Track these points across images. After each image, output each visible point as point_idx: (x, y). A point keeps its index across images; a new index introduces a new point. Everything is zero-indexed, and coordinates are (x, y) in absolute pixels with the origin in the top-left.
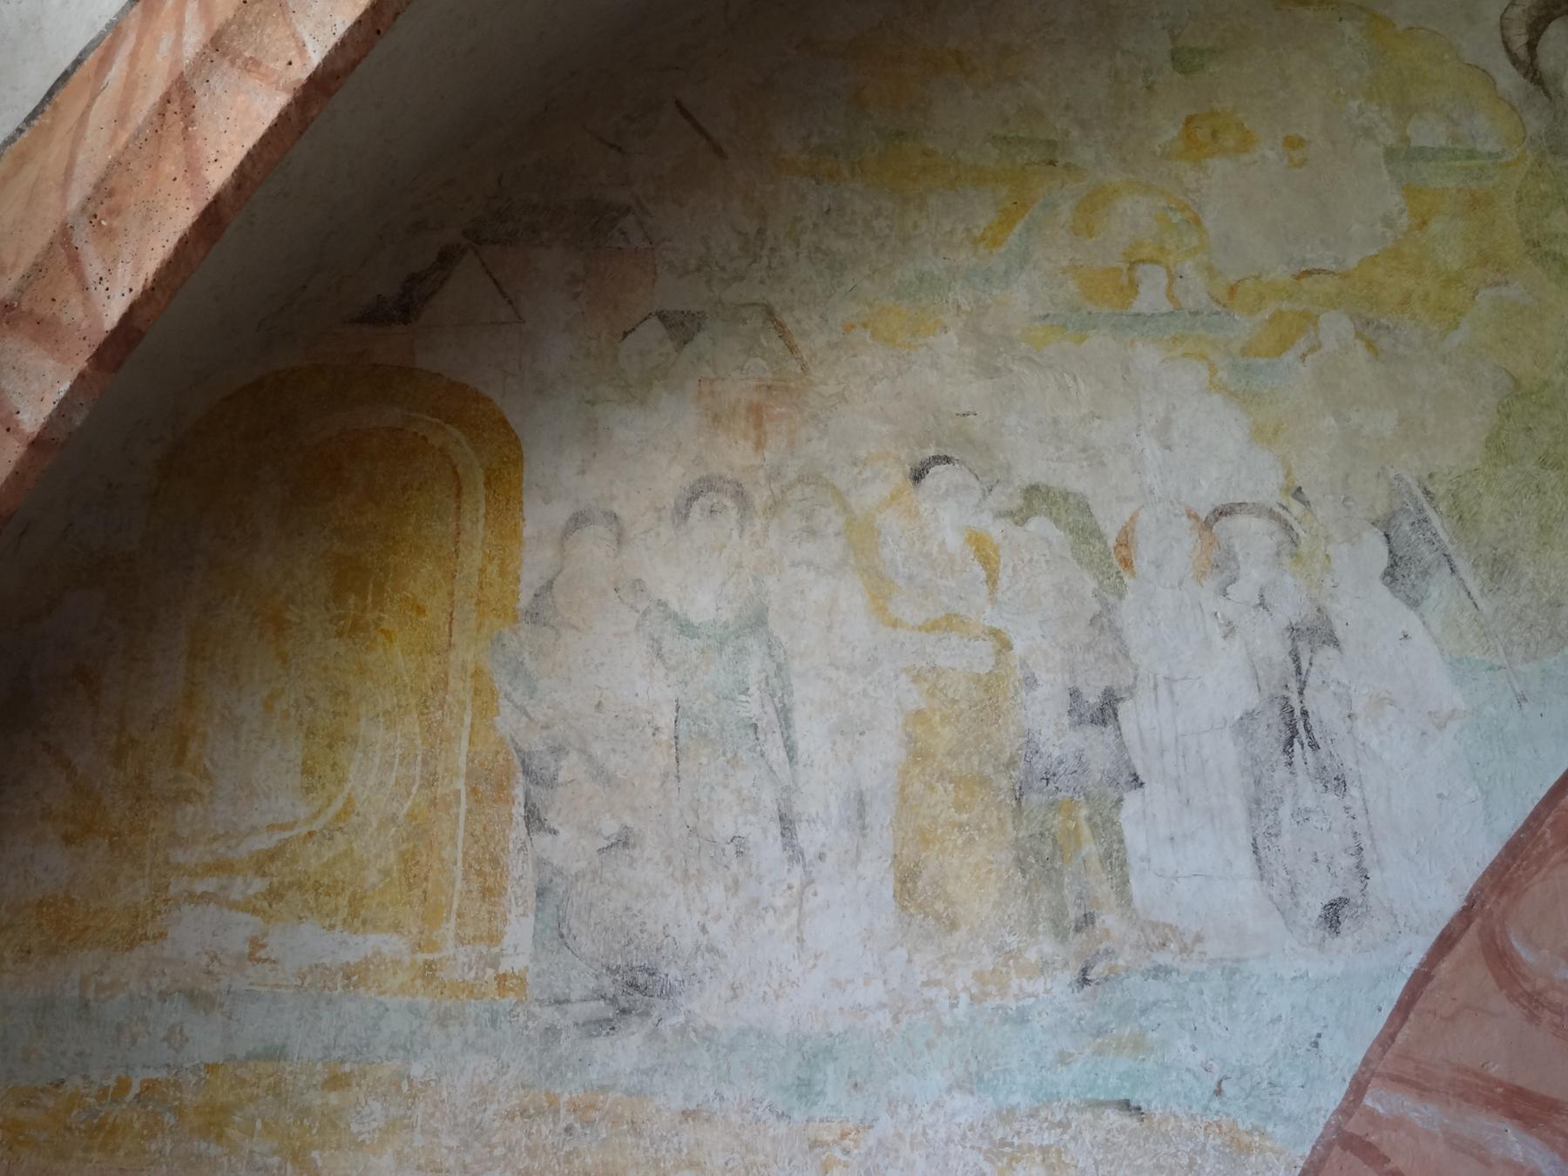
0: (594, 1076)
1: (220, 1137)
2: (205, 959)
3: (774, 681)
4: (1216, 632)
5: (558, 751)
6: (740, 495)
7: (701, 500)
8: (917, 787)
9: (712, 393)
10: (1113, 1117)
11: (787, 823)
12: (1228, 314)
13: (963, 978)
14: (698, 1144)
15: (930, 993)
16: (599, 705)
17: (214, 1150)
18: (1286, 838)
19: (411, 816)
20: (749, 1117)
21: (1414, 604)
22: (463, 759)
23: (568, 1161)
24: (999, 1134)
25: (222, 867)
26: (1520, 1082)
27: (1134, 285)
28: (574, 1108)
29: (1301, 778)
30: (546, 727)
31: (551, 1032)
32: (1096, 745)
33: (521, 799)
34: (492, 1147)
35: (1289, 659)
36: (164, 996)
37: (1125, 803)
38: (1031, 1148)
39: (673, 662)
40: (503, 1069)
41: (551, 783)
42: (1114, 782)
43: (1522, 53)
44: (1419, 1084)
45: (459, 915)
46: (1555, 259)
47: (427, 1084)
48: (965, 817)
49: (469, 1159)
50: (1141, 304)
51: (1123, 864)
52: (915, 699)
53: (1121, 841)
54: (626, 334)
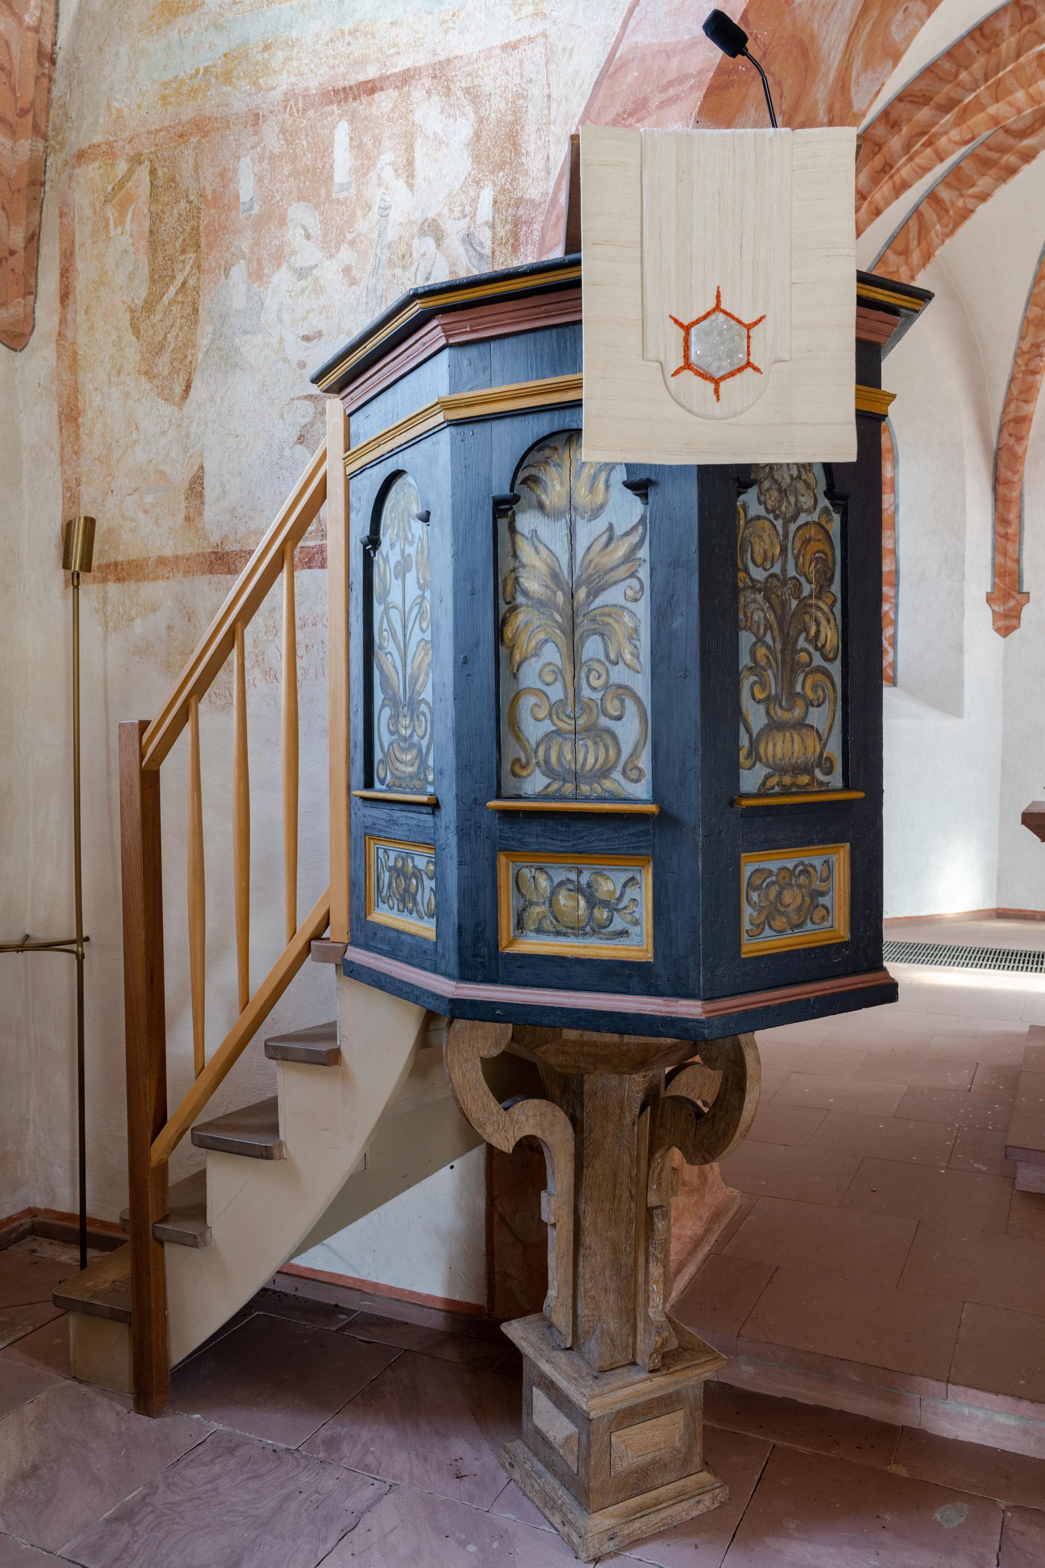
1: (230, 82)
14: (397, 36)
17: (229, 89)
28: (350, 33)
34: (321, 59)
36: (206, 29)
47: (297, 39)
49: (312, 66)
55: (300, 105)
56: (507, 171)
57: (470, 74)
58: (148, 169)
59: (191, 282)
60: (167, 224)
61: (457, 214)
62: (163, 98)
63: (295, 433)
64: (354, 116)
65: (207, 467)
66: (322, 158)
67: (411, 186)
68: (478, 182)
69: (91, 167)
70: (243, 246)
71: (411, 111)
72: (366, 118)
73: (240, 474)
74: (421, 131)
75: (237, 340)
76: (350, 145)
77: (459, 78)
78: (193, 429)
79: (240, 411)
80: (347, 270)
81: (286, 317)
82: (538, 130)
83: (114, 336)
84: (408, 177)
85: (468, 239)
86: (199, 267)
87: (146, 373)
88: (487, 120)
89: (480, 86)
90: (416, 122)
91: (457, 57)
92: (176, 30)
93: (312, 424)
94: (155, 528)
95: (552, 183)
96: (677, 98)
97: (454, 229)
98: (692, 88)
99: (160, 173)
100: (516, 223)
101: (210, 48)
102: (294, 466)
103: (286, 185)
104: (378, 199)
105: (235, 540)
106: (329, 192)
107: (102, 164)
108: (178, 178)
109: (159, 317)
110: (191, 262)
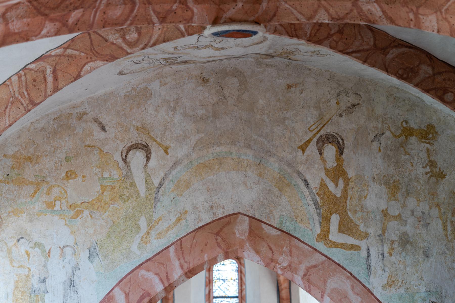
8: (16, 293)
18: (68, 301)
21: (92, 262)
27: (55, 205)
29: (72, 291)
32: (42, 286)
35: (72, 272)
37: (46, 295)
42: (44, 292)
43: (124, 158)
48: (22, 297)
50: (55, 209)
52: (16, 279)
53: (45, 301)
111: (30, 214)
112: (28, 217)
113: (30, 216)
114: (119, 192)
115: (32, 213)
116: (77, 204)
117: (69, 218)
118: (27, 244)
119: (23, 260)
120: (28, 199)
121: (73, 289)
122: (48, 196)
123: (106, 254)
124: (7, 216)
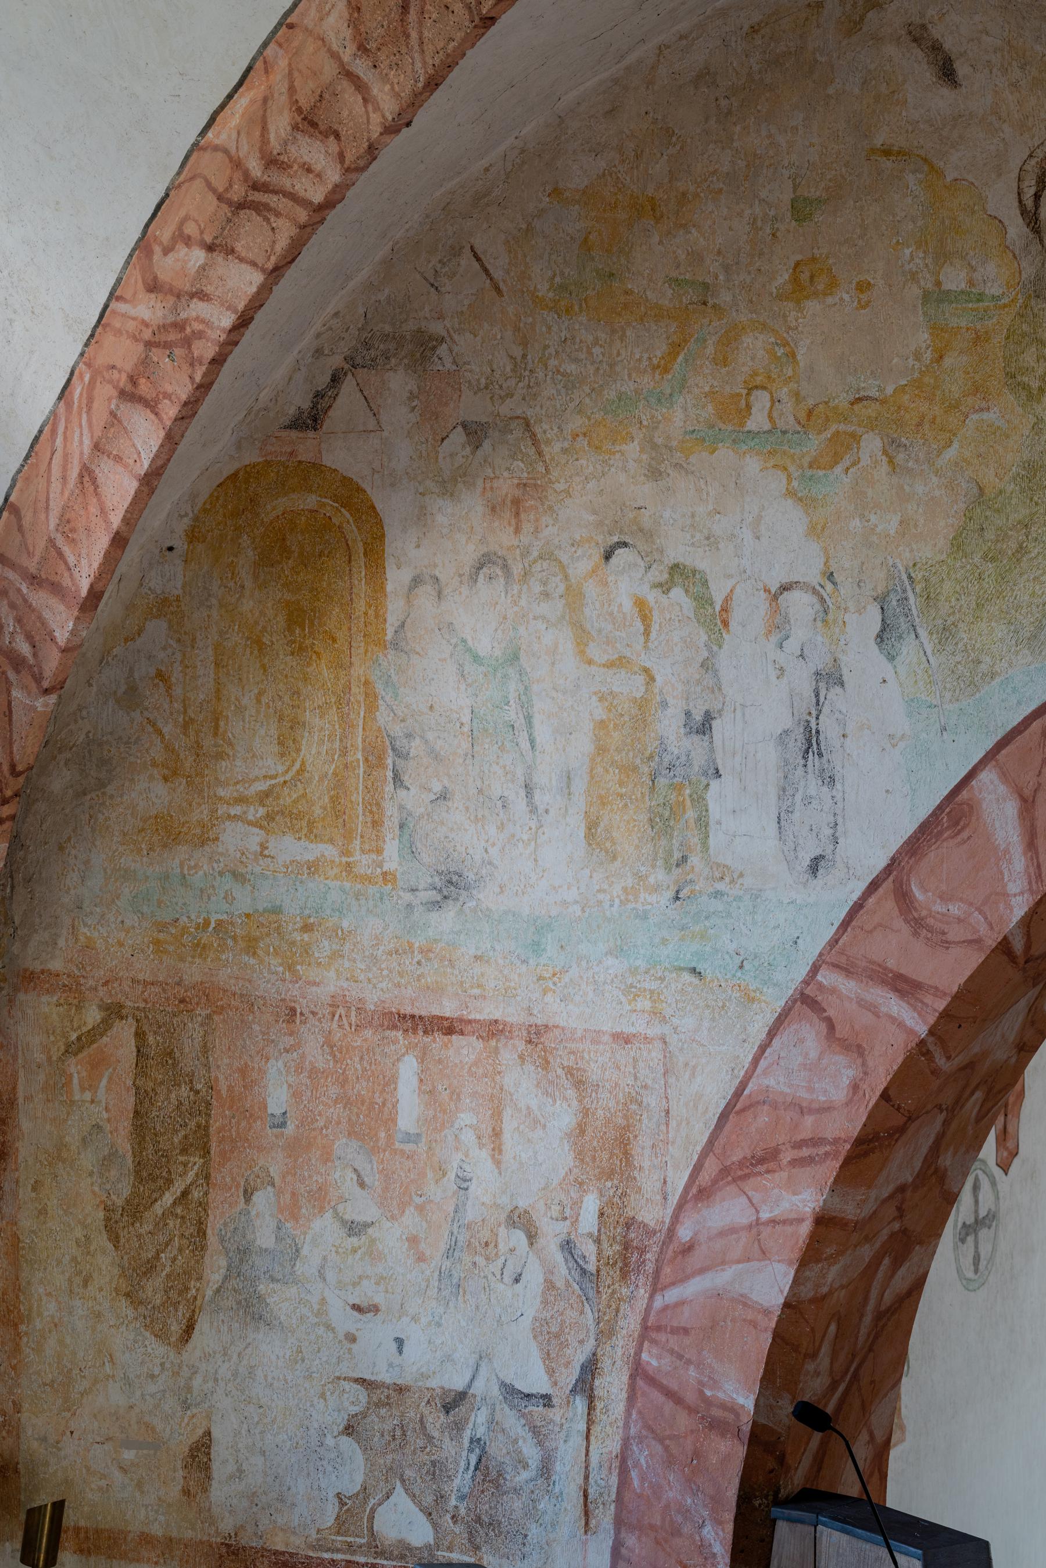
0: (431, 934)
1: (254, 953)
2: (239, 855)
3: (523, 698)
4: (773, 674)
5: (409, 736)
6: (506, 567)
7: (485, 569)
8: (599, 770)
9: (492, 488)
10: (687, 977)
11: (529, 789)
12: (805, 433)
13: (617, 890)
15: (601, 896)
16: (431, 707)
17: (252, 961)
18: (796, 816)
19: (335, 774)
20: (507, 961)
21: (891, 658)
22: (360, 739)
23: (419, 980)
24: (629, 981)
25: (241, 800)
26: (902, 971)
29: (810, 776)
30: (403, 721)
31: (409, 906)
32: (697, 746)
33: (391, 767)
34: (382, 970)
35: (813, 695)
36: (221, 874)
37: (711, 787)
38: (645, 990)
39: (469, 681)
40: (386, 927)
41: (405, 757)
42: (705, 774)
44: (848, 970)
45: (362, 837)
46: (1024, 388)
49: (371, 976)
51: (707, 825)
52: (600, 713)
53: (707, 811)
54: (443, 440)
55: (353, 1019)
56: (615, 1182)
57: (573, 1053)
58: (133, 1030)
59: (196, 1194)
60: (160, 1109)
61: (555, 1214)
62: (157, 942)
63: (342, 1421)
64: (425, 1054)
65: (214, 1434)
66: (381, 1093)
67: (498, 1163)
68: (581, 1184)
69: (45, 999)
70: (271, 1169)
71: (499, 1073)
72: (440, 1061)
73: (263, 1453)
74: (512, 1100)
75: (262, 1286)
76: (419, 1088)
77: (560, 1053)
78: (197, 1382)
79: (266, 1376)
80: (413, 1240)
81: (331, 1275)
82: (653, 1146)
83: (79, 1233)
84: (493, 1150)
85: (568, 1246)
86: (207, 1177)
87: (127, 1295)
88: (594, 1114)
89: (585, 1071)
90: (506, 1087)
91: (557, 1027)
92: (177, 861)
93: (364, 1415)
94: (137, 1494)
95: (670, 1211)
96: (810, 1161)
97: (552, 1232)
98: (827, 1154)
99: (151, 1039)
100: (626, 1246)
101: (225, 898)
102: (339, 1460)
103: (332, 1110)
104: (455, 1166)
105: (256, 1534)
106: (390, 1137)
107: (62, 1001)
108: (177, 1055)
109: (147, 1227)
110: (196, 1168)
111: (654, 446)
112: (644, 457)
113: (654, 455)
114: (1004, 358)
115: (659, 441)
116: (836, 408)
117: (801, 467)
118: (642, 570)
119: (624, 635)
120: (646, 381)
121: (817, 764)
122: (724, 370)
123: (949, 622)
124: (565, 451)
